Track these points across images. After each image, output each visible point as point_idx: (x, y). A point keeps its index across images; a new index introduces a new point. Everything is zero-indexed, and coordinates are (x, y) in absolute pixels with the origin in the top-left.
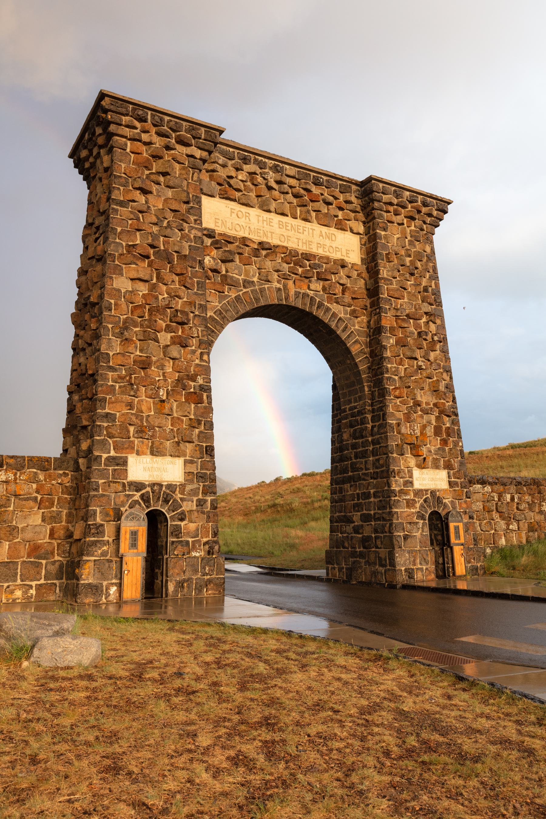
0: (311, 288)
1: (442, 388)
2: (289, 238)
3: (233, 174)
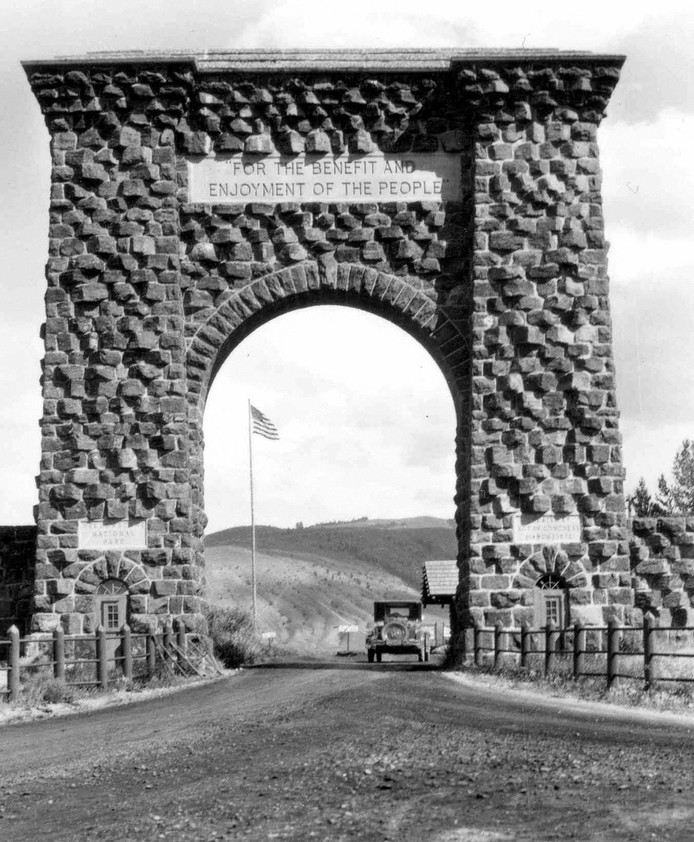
0: (365, 256)
1: (581, 382)
2: (330, 186)
3: (230, 113)
